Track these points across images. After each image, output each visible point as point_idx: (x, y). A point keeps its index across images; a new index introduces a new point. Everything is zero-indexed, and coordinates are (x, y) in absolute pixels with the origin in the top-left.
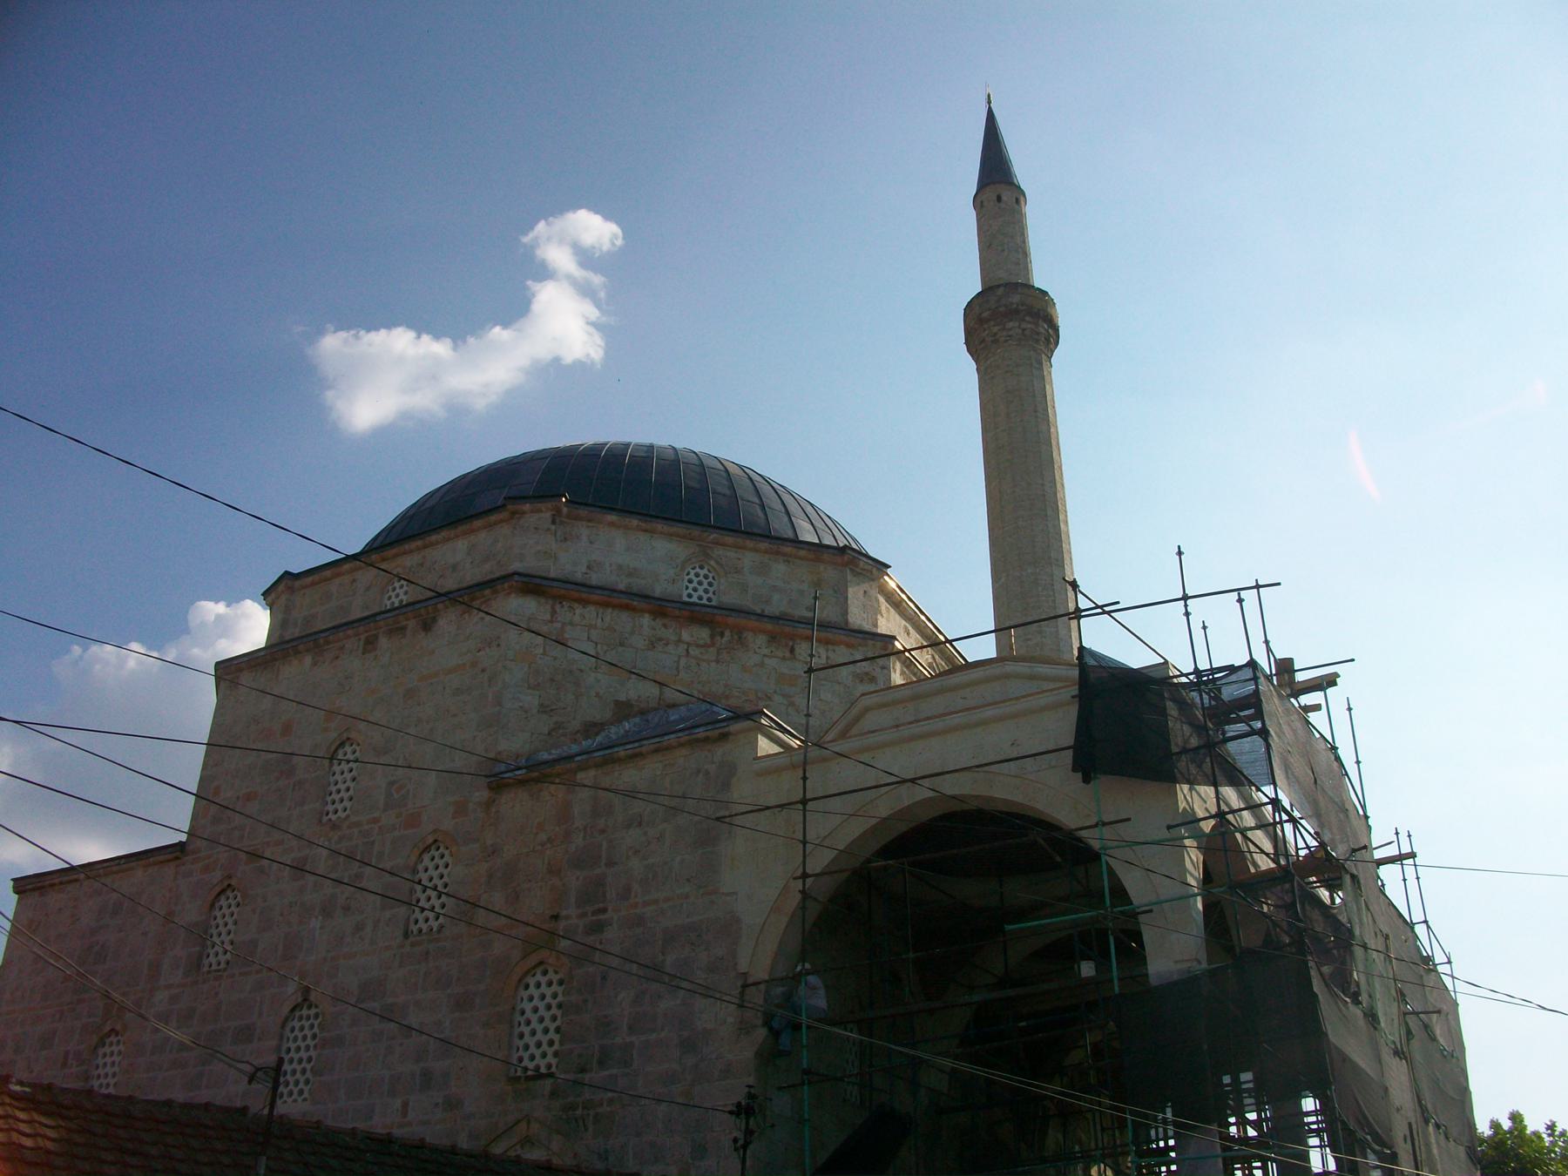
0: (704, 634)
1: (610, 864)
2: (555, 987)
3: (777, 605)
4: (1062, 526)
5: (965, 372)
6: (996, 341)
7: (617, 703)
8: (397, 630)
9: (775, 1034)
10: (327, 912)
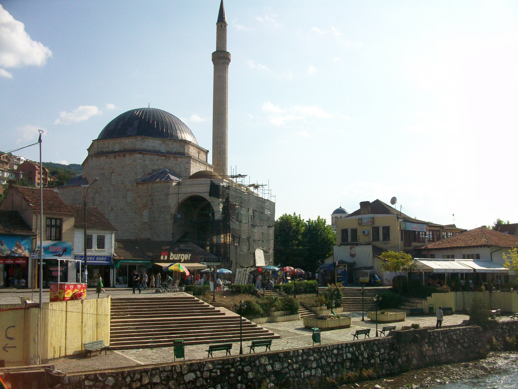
0: (164, 158)
1: (154, 197)
2: (147, 212)
3: (175, 150)
4: (226, 106)
5: (211, 66)
6: (217, 63)
8: (119, 156)
9: (175, 220)
10: (114, 198)
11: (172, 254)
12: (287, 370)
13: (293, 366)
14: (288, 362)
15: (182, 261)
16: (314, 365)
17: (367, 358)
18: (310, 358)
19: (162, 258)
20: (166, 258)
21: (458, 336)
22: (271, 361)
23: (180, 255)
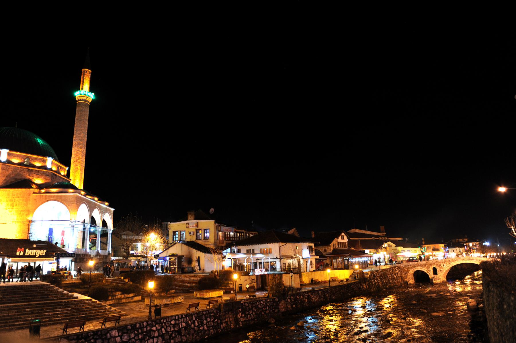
1: (14, 201)
7: (15, 179)
11: (27, 250)
12: (134, 340)
13: (139, 337)
14: (135, 333)
15: (37, 256)
16: (156, 334)
17: (197, 326)
18: (152, 329)
19: (18, 254)
20: (22, 253)
21: (262, 305)
22: (120, 334)
23: (36, 251)
